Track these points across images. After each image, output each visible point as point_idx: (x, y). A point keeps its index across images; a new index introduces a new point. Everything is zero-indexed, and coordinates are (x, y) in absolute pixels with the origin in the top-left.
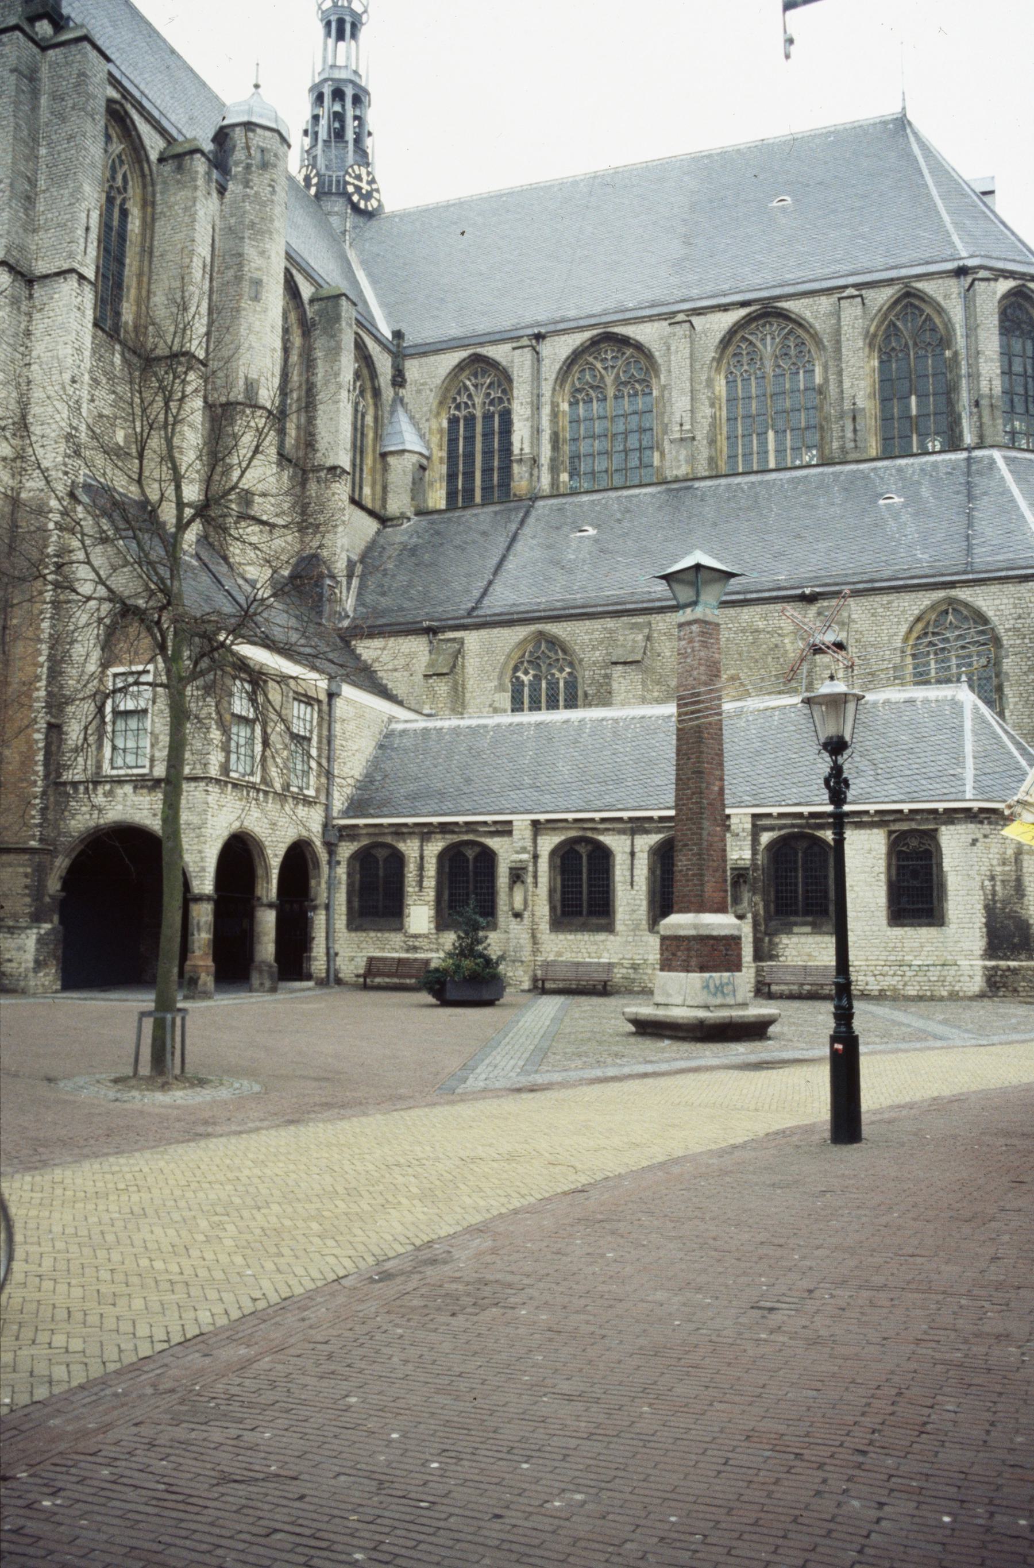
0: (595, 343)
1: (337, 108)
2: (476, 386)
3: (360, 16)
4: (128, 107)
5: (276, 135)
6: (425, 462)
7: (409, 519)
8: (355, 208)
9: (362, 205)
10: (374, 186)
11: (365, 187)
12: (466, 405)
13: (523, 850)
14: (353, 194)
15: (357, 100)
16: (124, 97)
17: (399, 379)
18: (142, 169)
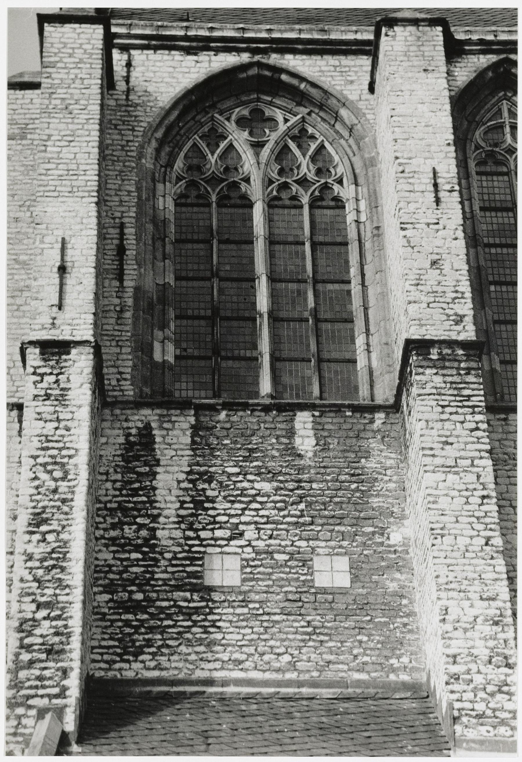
16: (254, 52)
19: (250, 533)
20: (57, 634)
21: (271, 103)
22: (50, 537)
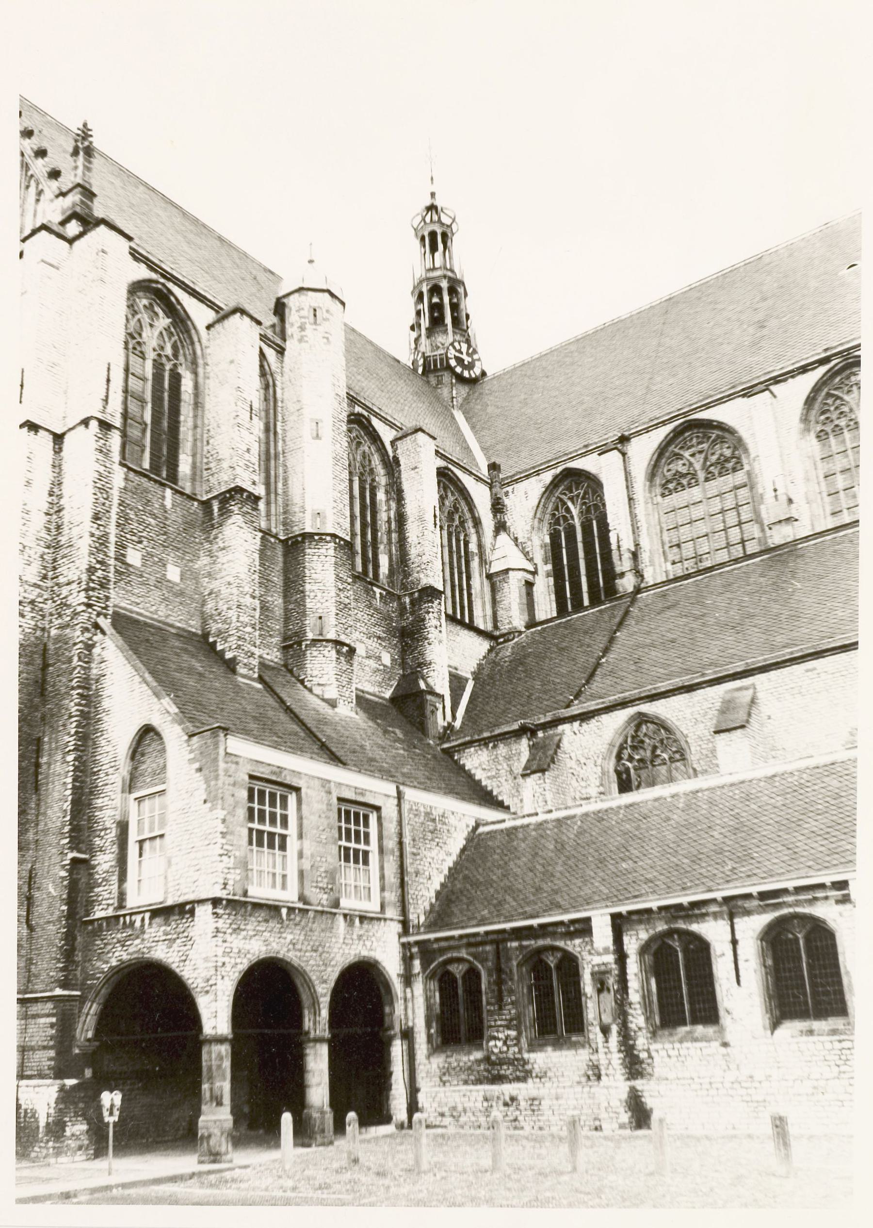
0: (677, 433)
1: (435, 300)
2: (571, 499)
3: (450, 226)
4: (170, 285)
5: (327, 295)
6: (530, 577)
7: (520, 633)
8: (460, 379)
9: (466, 374)
10: (475, 357)
11: (467, 359)
12: (564, 517)
13: (606, 951)
14: (462, 372)
15: (452, 291)
17: (498, 507)
18: (190, 338)
19: (145, 543)
20: (104, 578)
21: (159, 305)
22: (102, 528)
